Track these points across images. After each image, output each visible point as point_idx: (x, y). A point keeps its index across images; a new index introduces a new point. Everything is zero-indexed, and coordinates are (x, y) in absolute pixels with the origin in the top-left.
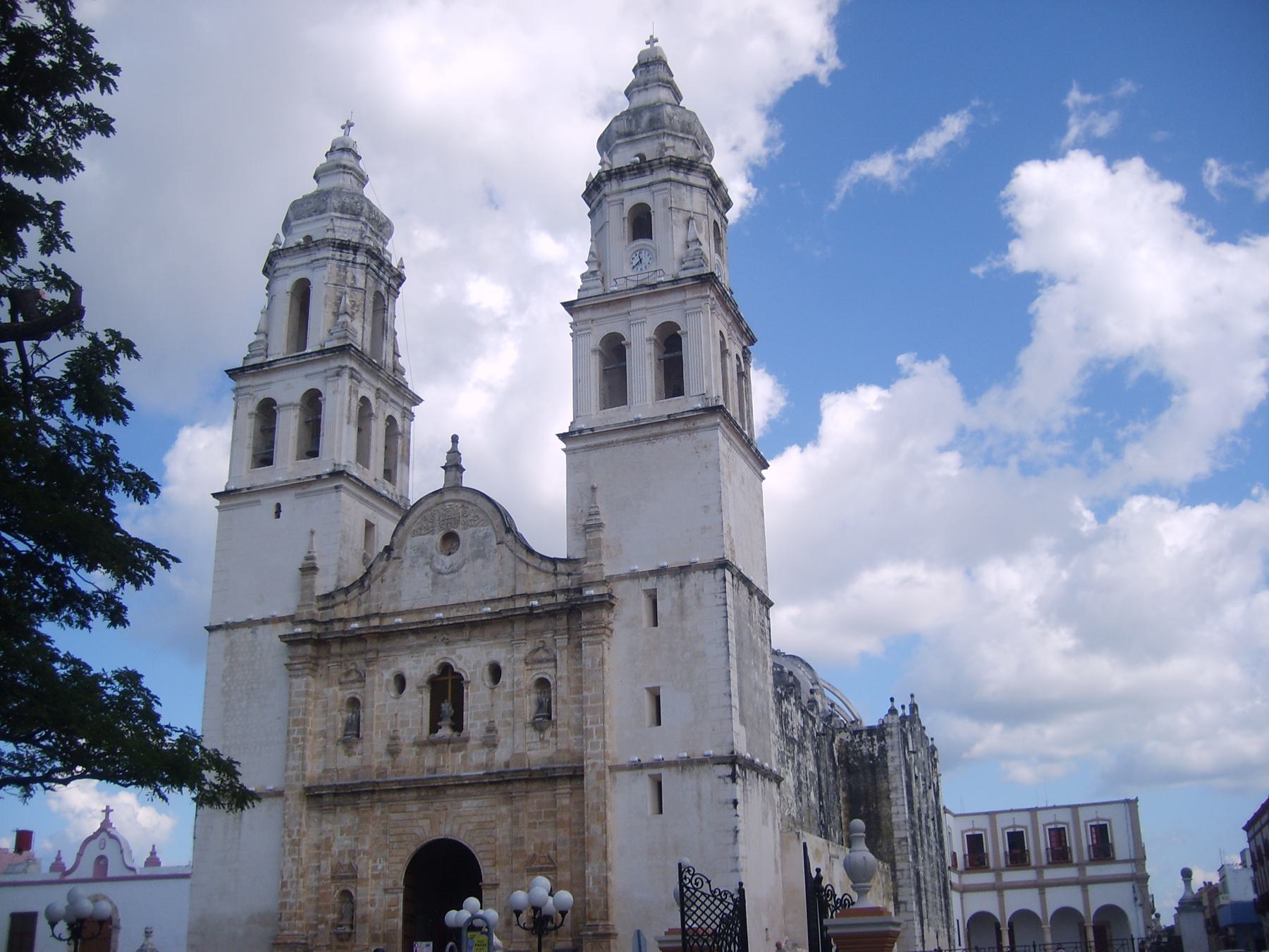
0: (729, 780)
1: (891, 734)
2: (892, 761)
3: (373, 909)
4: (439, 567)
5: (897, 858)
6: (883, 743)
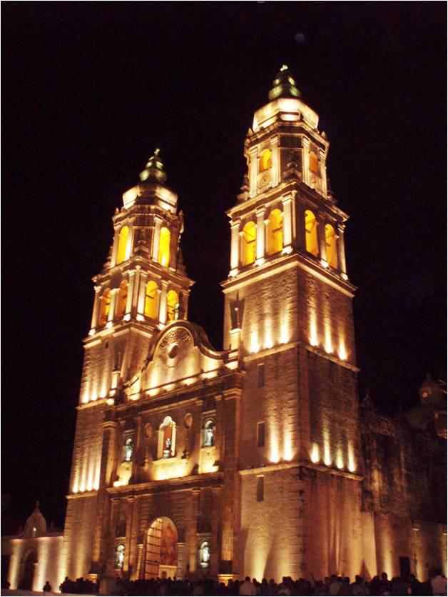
0: (298, 477)
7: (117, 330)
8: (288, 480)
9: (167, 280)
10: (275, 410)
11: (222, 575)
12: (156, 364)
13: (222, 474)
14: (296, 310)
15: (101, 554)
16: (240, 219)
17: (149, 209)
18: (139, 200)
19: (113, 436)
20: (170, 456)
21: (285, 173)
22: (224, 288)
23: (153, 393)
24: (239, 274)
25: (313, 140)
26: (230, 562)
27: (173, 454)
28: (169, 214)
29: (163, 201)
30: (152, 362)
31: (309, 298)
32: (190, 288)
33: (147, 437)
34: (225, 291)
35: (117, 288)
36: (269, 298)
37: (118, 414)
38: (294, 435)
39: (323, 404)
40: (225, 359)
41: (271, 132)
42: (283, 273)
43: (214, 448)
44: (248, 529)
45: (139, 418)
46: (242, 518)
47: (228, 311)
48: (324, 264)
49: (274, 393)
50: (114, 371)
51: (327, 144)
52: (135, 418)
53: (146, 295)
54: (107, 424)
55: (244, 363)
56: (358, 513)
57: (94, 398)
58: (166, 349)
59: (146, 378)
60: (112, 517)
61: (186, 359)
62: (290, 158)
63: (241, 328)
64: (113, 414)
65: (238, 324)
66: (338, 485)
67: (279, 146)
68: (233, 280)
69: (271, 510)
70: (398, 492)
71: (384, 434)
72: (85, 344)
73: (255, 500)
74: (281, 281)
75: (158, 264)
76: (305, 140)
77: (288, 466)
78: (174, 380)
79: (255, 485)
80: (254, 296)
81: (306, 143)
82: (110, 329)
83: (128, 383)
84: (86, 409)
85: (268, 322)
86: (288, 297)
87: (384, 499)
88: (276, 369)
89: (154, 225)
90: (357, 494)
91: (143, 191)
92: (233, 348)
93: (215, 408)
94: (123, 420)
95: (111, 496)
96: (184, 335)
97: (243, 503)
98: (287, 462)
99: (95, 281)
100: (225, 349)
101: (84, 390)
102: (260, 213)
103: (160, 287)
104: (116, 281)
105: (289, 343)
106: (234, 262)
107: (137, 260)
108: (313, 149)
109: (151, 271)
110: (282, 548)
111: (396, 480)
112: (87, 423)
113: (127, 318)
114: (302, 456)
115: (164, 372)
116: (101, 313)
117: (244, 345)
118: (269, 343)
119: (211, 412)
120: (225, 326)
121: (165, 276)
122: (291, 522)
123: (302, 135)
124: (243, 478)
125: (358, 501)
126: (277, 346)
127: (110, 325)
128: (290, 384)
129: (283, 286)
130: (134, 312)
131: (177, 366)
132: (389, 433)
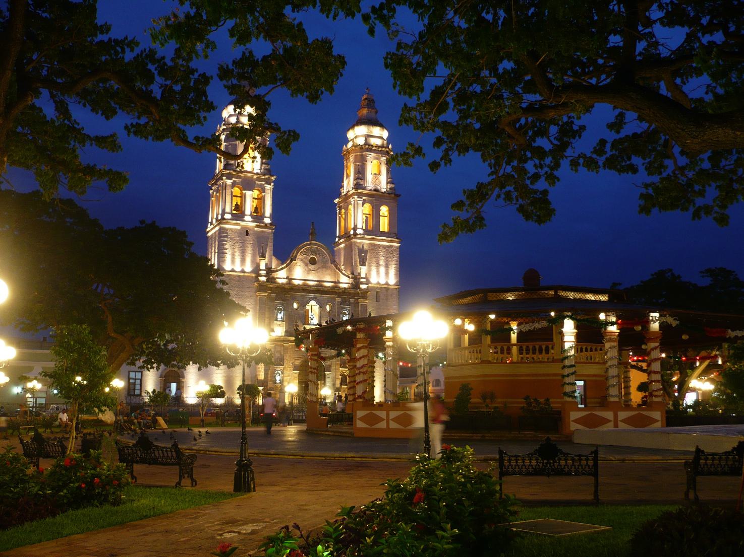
4: (310, 268)
7: (257, 226)
12: (298, 264)
24: (364, 234)
42: (391, 246)
61: (324, 269)
80: (374, 251)
85: (382, 269)
118: (383, 281)
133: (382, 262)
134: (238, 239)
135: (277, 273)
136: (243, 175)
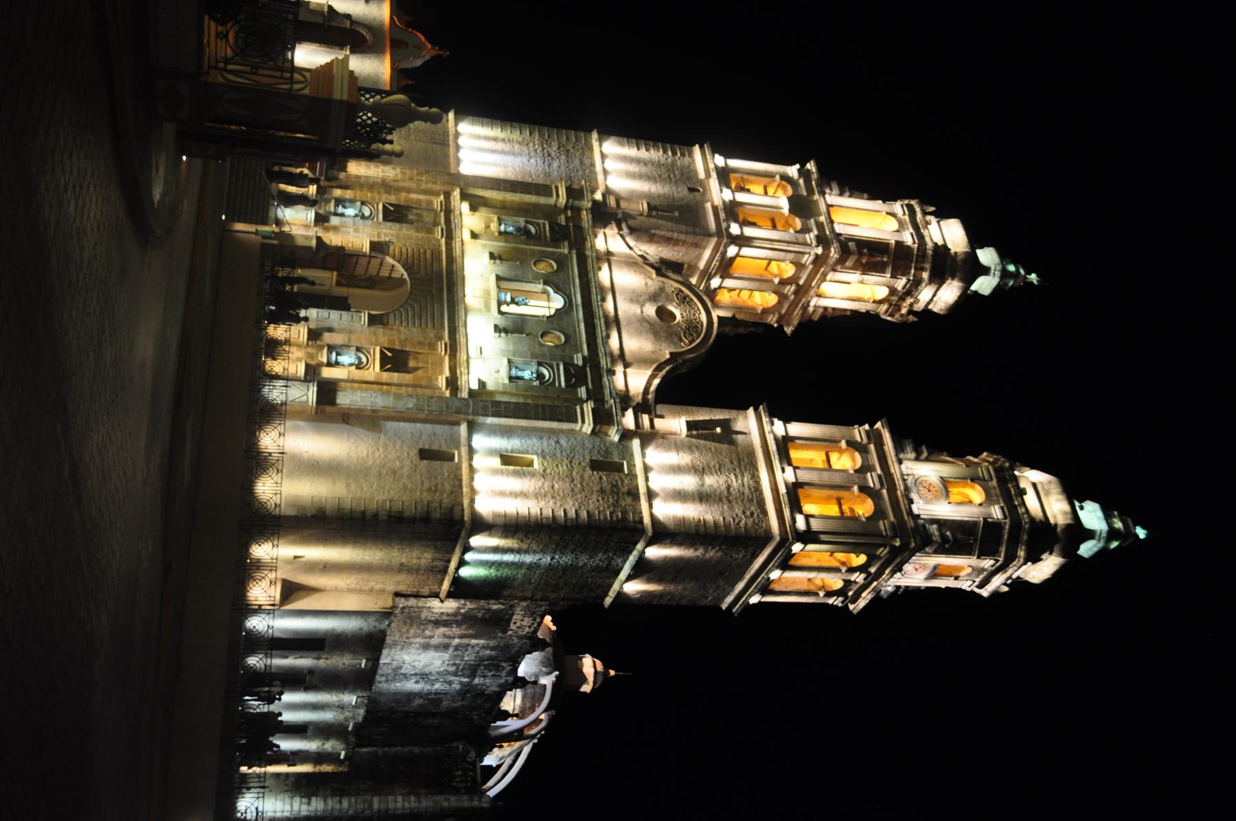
1: (472, 800)
2: (445, 799)
3: (351, 230)
5: (353, 799)
6: (463, 791)
8: (446, 501)
9: (796, 293)
10: (553, 487)
11: (315, 389)
12: (650, 282)
13: (465, 394)
14: (702, 529)
15: (357, 177)
16: (869, 443)
17: (923, 269)
18: (942, 251)
19: (542, 200)
20: (500, 304)
21: (935, 526)
22: (756, 410)
23: (604, 276)
24: (776, 438)
25: (993, 574)
26: (332, 402)
27: (504, 308)
28: (912, 300)
29: (938, 290)
30: (654, 275)
31: (721, 550)
32: (781, 327)
33: (535, 265)
34: (751, 411)
35: (791, 211)
36: (728, 488)
37: (577, 211)
38: (511, 516)
39: (557, 557)
40: (643, 407)
41: (1015, 507)
42: (764, 512)
43: (507, 381)
44: (380, 431)
45: (566, 251)
46: (397, 423)
47: (719, 415)
48: (775, 575)
49: (579, 486)
50: (649, 204)
51: (985, 592)
52: (566, 243)
53: (770, 260)
54: (562, 192)
55: (631, 439)
56: (392, 588)
57: (609, 165)
58: (671, 300)
59: (632, 263)
60: (414, 196)
61: (651, 337)
62: (959, 536)
63: (687, 436)
64: (577, 203)
65: (694, 432)
66: (433, 567)
67: (985, 519)
68: (767, 428)
69: (406, 471)
70: (424, 631)
71: (513, 621)
72: (702, 147)
73: (421, 447)
74: (753, 509)
75: (823, 279)
76: (992, 562)
77: (466, 502)
78: (620, 313)
79: (444, 448)
80: (735, 463)
81: (987, 563)
82: (719, 195)
83: (625, 231)
84: (591, 149)
85: (689, 482)
86: (724, 518)
87: (415, 612)
88: (615, 490)
89: (893, 276)
90: (421, 590)
91: (959, 258)
92: (657, 422)
93: (566, 386)
94: (567, 219)
95: (448, 195)
96: (692, 335)
97: (419, 425)
98: (472, 501)
99: (808, 166)
100: (659, 407)
101: (622, 144)
102: (872, 480)
103: (784, 282)
104: (802, 206)
105: (652, 516)
106: (796, 429)
107: (832, 249)
108: (977, 571)
109: (812, 270)
110: (348, 485)
111: (442, 630)
112: (568, 151)
113: (735, 229)
114: (480, 525)
115: (636, 298)
116: (753, 178)
117: (660, 441)
118: (658, 482)
119: (562, 378)
120: (693, 408)
121: (802, 291)
122: (385, 501)
123: (1001, 559)
124: (455, 428)
125: (409, 590)
126: (651, 495)
127: (727, 195)
128: (588, 512)
129: (744, 513)
130: (742, 241)
131: (643, 320)
132: (513, 627)
133: (711, 481)
134: (677, 173)
135: (618, 237)
136: (816, 197)
